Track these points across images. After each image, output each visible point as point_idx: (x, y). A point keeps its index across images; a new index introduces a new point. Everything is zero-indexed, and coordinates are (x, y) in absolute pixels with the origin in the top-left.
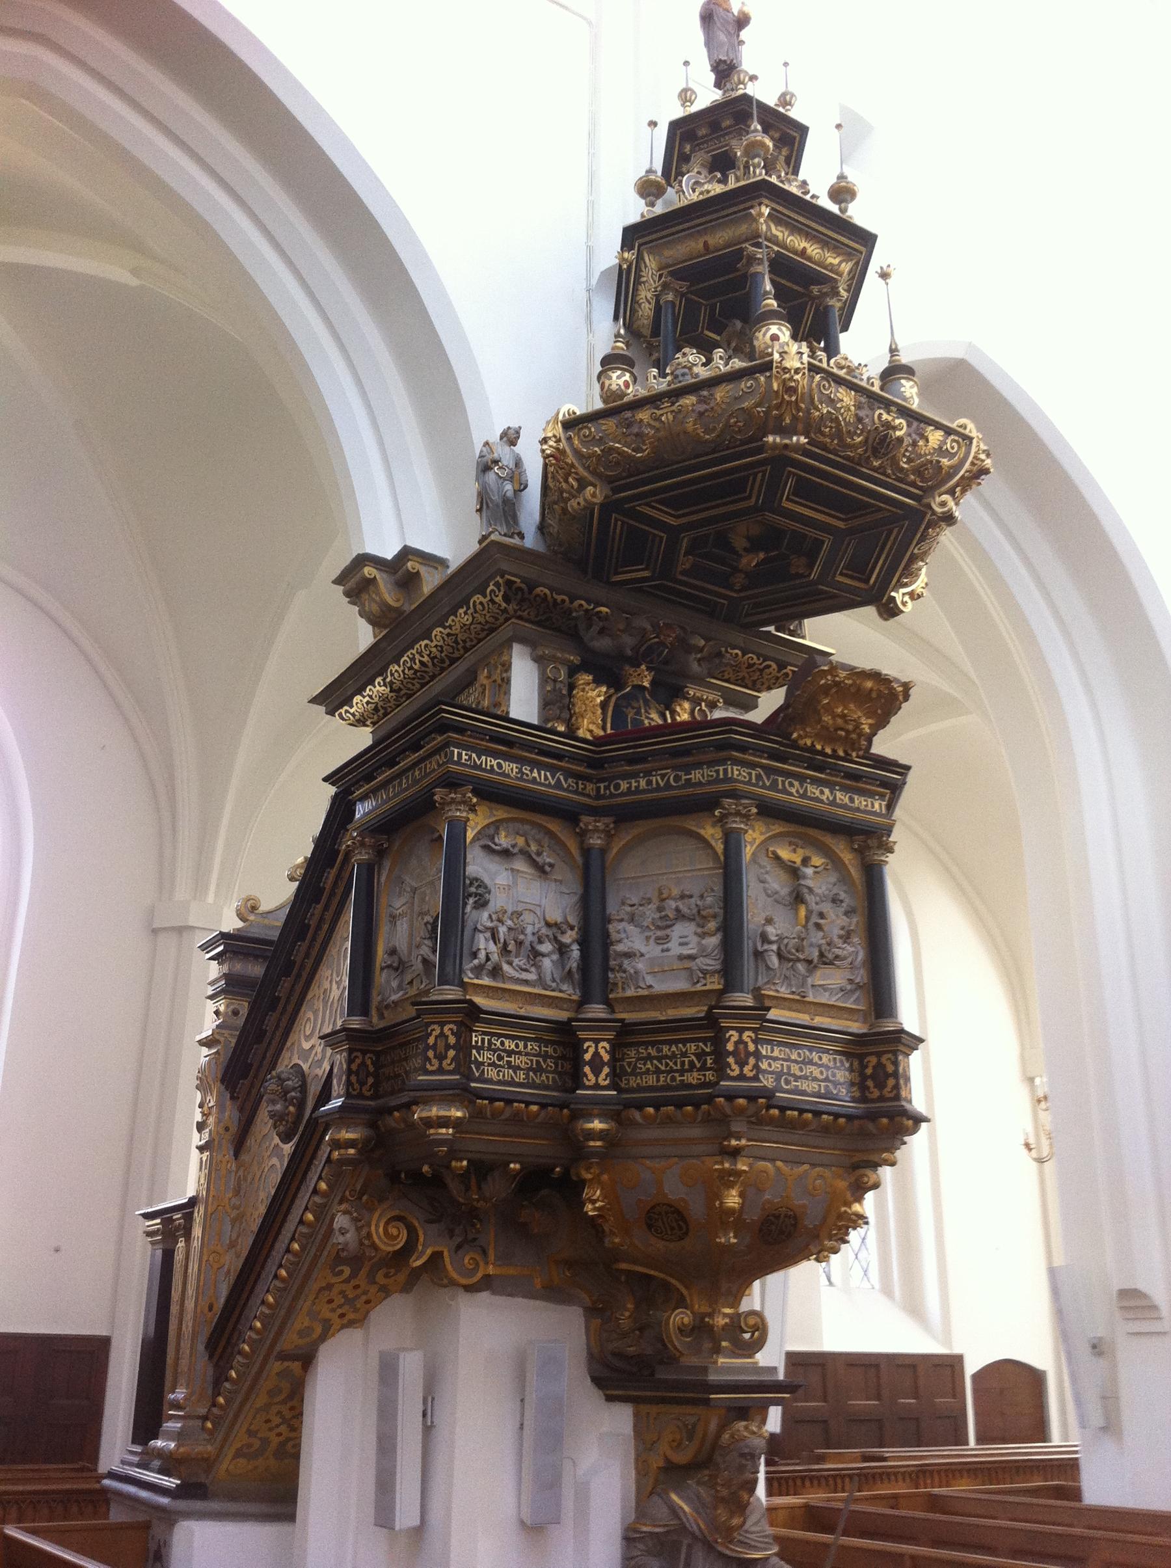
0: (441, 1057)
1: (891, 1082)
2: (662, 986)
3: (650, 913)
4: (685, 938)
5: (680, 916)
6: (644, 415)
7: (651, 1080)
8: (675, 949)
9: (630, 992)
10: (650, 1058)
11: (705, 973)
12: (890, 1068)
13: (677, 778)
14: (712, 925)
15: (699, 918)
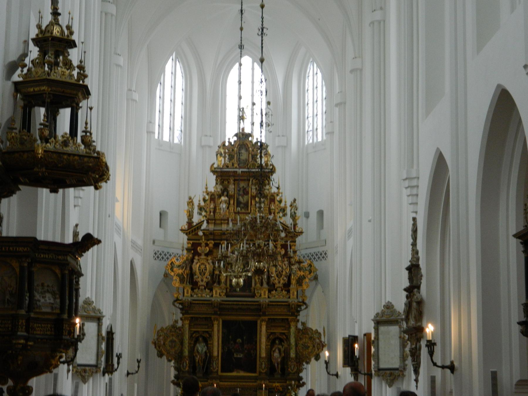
0: (22, 328)
1: (72, 334)
2: (44, 310)
3: (40, 289)
4: (49, 299)
5: (48, 291)
6: (65, 157)
7: (39, 333)
8: (48, 301)
9: (37, 310)
10: (39, 327)
11: (56, 308)
12: (72, 331)
13: (55, 257)
14: (57, 296)
15: (53, 294)
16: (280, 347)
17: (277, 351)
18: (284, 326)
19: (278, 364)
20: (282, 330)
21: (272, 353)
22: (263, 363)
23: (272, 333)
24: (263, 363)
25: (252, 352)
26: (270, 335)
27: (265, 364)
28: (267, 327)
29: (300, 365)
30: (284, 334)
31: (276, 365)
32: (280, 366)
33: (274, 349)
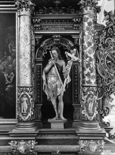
16: (62, 63)
17: (55, 70)
18: (70, 21)
19: (58, 101)
20: (67, 29)
21: (44, 77)
22: (25, 99)
23: (45, 36)
24: (25, 99)
25: (6, 75)
26: (41, 41)
27: (28, 102)
28: (32, 23)
29: (103, 99)
30: (69, 37)
31: (54, 102)
32: (62, 104)
33: (47, 68)
